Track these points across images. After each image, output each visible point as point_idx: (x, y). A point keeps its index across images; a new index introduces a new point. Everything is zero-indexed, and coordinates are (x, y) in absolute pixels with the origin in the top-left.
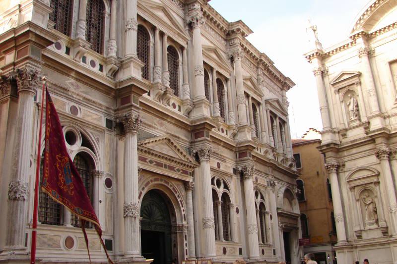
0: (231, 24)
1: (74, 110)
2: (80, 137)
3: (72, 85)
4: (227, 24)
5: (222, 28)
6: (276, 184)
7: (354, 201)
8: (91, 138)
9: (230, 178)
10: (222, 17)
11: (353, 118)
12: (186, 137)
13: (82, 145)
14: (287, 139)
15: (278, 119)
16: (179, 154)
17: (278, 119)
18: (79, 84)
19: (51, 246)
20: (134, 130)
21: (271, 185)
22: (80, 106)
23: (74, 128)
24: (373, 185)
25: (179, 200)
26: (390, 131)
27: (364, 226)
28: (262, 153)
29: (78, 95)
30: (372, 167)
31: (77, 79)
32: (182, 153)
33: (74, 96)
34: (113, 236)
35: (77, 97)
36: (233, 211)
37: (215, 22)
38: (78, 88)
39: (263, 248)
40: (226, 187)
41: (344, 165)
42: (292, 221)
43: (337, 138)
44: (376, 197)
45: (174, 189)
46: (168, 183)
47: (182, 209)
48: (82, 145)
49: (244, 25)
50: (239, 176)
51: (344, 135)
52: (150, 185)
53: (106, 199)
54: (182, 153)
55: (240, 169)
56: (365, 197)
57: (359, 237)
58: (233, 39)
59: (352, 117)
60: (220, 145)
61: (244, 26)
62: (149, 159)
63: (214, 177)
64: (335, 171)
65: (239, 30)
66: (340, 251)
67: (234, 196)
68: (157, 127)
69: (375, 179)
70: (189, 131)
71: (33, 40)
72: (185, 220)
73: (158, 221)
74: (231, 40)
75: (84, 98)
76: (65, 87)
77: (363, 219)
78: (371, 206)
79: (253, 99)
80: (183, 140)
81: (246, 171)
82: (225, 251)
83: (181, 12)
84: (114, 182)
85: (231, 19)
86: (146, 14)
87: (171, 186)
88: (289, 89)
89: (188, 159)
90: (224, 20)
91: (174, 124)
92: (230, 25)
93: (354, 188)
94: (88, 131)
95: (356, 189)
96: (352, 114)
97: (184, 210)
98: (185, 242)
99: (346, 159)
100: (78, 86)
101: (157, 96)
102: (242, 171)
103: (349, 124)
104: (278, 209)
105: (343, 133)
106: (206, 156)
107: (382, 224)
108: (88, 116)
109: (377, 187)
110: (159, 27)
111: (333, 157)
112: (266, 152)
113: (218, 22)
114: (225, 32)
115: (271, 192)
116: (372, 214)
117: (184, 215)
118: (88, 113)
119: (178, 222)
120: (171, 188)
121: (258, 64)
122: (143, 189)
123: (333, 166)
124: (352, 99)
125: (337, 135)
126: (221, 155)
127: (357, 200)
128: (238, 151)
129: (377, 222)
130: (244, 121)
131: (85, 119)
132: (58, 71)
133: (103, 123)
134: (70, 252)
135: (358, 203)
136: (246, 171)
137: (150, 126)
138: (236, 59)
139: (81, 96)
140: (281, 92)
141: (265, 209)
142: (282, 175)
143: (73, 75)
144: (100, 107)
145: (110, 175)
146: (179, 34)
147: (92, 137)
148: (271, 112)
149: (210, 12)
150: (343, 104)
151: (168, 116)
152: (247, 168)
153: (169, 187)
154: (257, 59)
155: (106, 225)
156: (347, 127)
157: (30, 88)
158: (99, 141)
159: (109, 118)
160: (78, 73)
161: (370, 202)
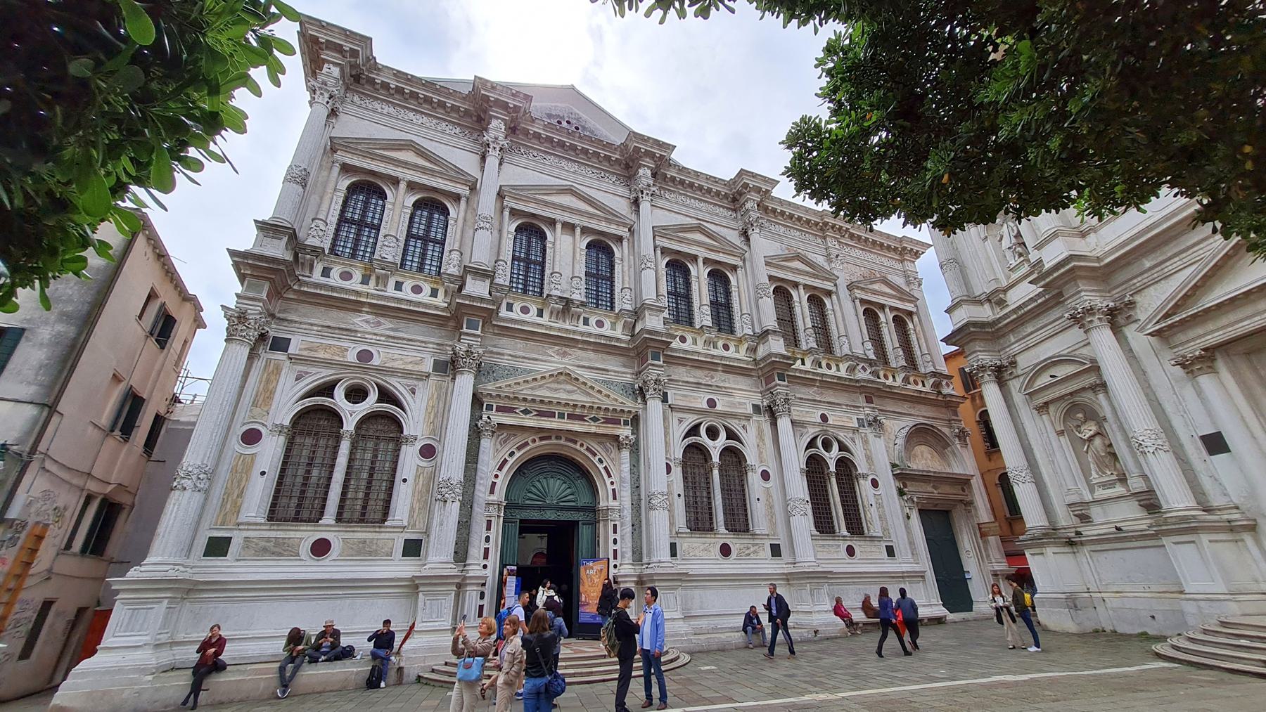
0: (731, 183)
1: (365, 356)
2: (374, 391)
3: (367, 322)
4: (725, 185)
5: (718, 194)
6: (884, 421)
7: (1053, 435)
8: (397, 390)
9: (744, 423)
10: (711, 176)
11: (1013, 262)
12: (625, 366)
13: (377, 402)
14: (922, 341)
15: (887, 310)
16: (598, 396)
17: (887, 310)
18: (382, 320)
19: (279, 554)
20: (462, 367)
21: (870, 425)
22: (378, 349)
23: (366, 380)
24: (1090, 395)
25: (601, 467)
26: (1098, 259)
27: (1092, 491)
28: (843, 373)
29: (375, 334)
30: (1077, 352)
31: (375, 314)
32: (600, 392)
33: (367, 336)
34: (427, 533)
35: (374, 337)
36: (754, 479)
37: (701, 188)
38: (379, 324)
39: (849, 543)
40: (731, 435)
41: (1013, 363)
42: (957, 490)
43: (986, 313)
44: (1105, 419)
45: (588, 449)
46: (575, 442)
47: (608, 481)
48: (377, 402)
49: (754, 175)
50: (766, 415)
51: (1001, 303)
52: (528, 448)
53: (417, 477)
54: (600, 392)
55: (765, 404)
56: (1079, 423)
57: (1085, 519)
58: (744, 204)
59: (1013, 262)
60: (717, 370)
61: (753, 177)
62: (523, 408)
63: (699, 424)
64: (993, 378)
65: (746, 186)
66: (1032, 551)
67: (755, 450)
68: (553, 359)
69: (1091, 379)
70: (632, 357)
71: (249, 272)
72: (615, 498)
73: (561, 504)
74: (741, 207)
75: (389, 337)
76: (352, 327)
77: (1086, 474)
78: (1098, 442)
79: (806, 286)
80: (615, 372)
81: (775, 405)
82: (725, 550)
83: (623, 191)
84: (438, 448)
85: (728, 174)
86: (533, 205)
87: (582, 445)
88: (917, 255)
89: (616, 400)
90: (716, 181)
91: (593, 350)
92: (734, 181)
93: (1046, 404)
94: (393, 381)
95: (1052, 409)
96: (1009, 254)
97: (612, 483)
98: (612, 537)
99: (1016, 348)
100: (379, 322)
101: (554, 315)
102: (769, 406)
103: (1008, 278)
104: (894, 466)
105: (996, 298)
106: (651, 391)
107: (1136, 484)
108: (397, 360)
109: (1101, 396)
110: (561, 216)
111: (980, 351)
112: (851, 369)
113: (706, 186)
114: (726, 196)
115: (871, 437)
116: (1107, 461)
117: (614, 490)
118: (396, 356)
119: (602, 504)
120: (582, 450)
121: (821, 229)
122: (512, 454)
123: (982, 368)
124: (1005, 225)
125: (987, 306)
126: (717, 386)
127: (1060, 433)
128: (763, 375)
129: (1123, 479)
130: (770, 320)
131: (387, 365)
132: (337, 307)
133: (428, 366)
134: (320, 563)
135: (1065, 440)
136: (775, 405)
137: (536, 360)
138: (750, 232)
139: (382, 335)
140: (898, 266)
141: (856, 469)
142: (909, 404)
143: (367, 310)
144: (423, 345)
145: (434, 439)
146: (607, 220)
147: (398, 386)
148: (863, 301)
149: (682, 175)
150: (988, 243)
151: (577, 341)
152: (775, 401)
153: (578, 447)
154: (817, 224)
155: (411, 515)
156: (1005, 284)
157: (233, 335)
158: (414, 393)
159: (443, 358)
160: (371, 305)
161: (1092, 433)
